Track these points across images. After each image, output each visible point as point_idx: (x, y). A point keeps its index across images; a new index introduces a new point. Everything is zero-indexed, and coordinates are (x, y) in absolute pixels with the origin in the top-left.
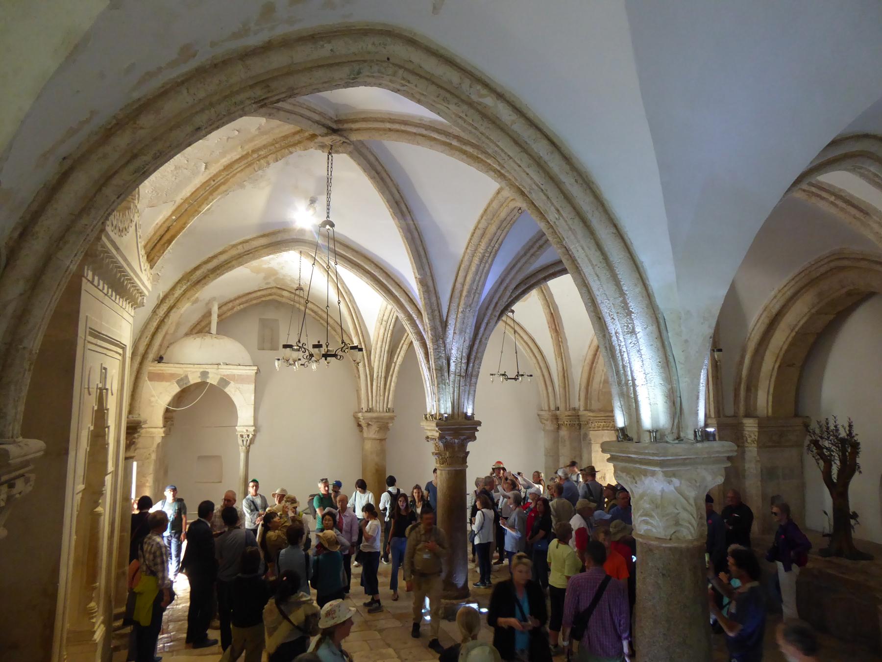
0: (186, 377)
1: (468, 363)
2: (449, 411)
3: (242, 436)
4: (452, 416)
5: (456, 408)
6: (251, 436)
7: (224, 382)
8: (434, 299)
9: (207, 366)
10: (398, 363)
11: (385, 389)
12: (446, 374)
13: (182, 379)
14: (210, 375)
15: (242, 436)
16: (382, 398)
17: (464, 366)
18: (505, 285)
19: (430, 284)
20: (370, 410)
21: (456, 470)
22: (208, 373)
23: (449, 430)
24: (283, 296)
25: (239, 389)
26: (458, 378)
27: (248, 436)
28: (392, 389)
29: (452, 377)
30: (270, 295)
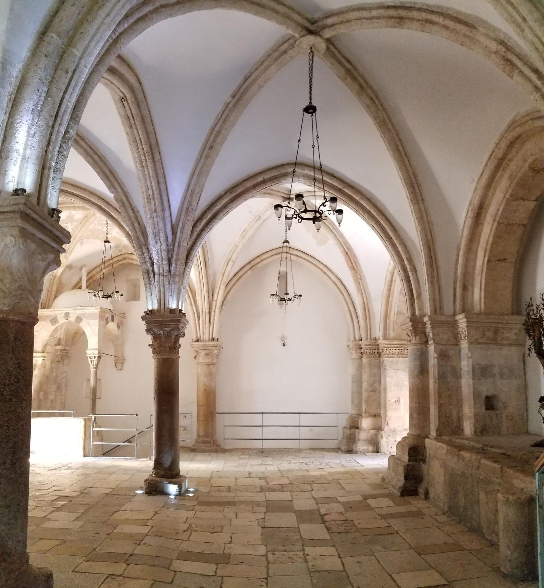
0: (56, 317)
1: (170, 266)
2: (156, 307)
3: (90, 358)
4: (159, 310)
5: (162, 303)
6: (97, 357)
7: (79, 319)
8: (130, 212)
9: (67, 309)
10: (218, 301)
11: (210, 322)
12: (152, 276)
13: (53, 319)
14: (70, 315)
15: (90, 358)
16: (208, 330)
17: (166, 268)
18: (190, 191)
19: (124, 199)
20: (198, 340)
21: (163, 358)
22: (69, 313)
23: (155, 322)
24: (133, 259)
25: (88, 323)
26: (162, 278)
27: (95, 357)
28: (215, 322)
29: (156, 276)
30: (125, 259)
